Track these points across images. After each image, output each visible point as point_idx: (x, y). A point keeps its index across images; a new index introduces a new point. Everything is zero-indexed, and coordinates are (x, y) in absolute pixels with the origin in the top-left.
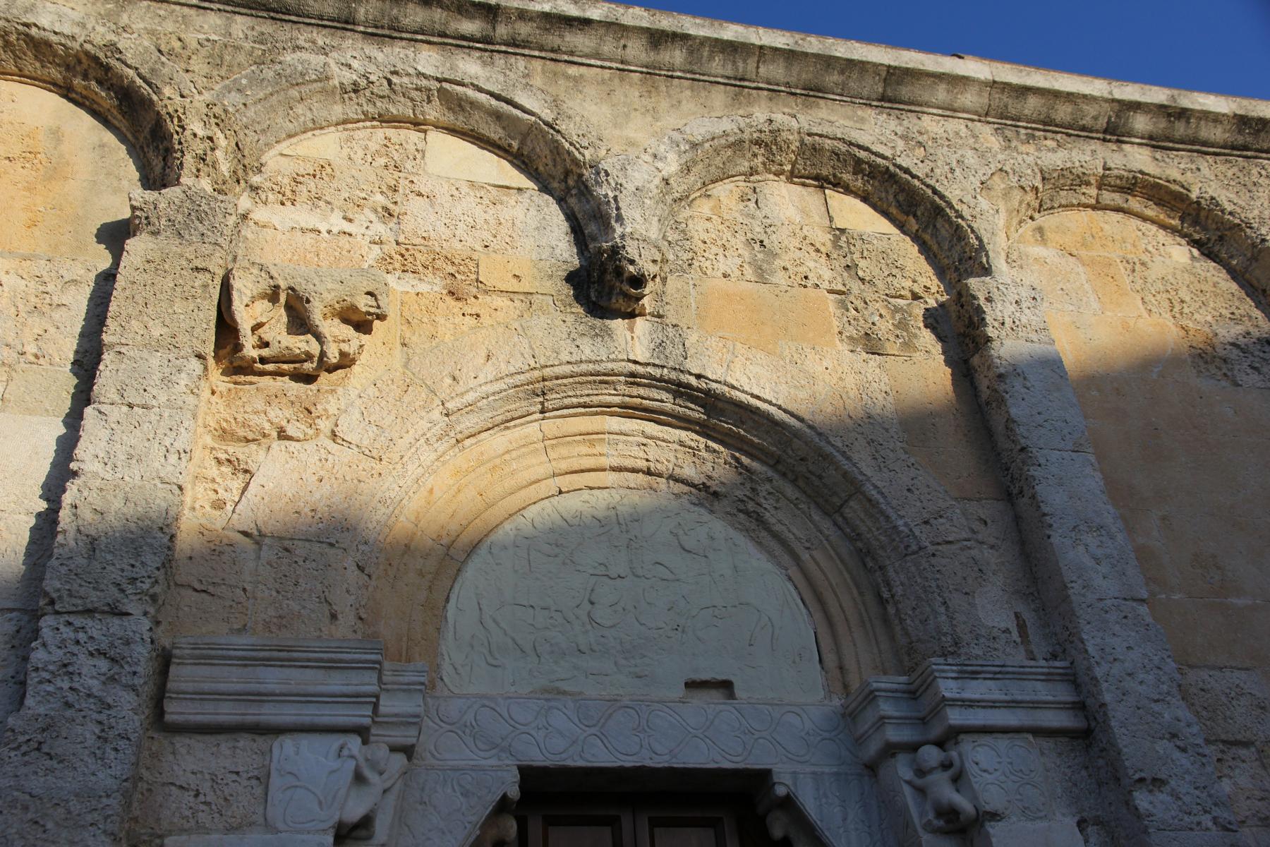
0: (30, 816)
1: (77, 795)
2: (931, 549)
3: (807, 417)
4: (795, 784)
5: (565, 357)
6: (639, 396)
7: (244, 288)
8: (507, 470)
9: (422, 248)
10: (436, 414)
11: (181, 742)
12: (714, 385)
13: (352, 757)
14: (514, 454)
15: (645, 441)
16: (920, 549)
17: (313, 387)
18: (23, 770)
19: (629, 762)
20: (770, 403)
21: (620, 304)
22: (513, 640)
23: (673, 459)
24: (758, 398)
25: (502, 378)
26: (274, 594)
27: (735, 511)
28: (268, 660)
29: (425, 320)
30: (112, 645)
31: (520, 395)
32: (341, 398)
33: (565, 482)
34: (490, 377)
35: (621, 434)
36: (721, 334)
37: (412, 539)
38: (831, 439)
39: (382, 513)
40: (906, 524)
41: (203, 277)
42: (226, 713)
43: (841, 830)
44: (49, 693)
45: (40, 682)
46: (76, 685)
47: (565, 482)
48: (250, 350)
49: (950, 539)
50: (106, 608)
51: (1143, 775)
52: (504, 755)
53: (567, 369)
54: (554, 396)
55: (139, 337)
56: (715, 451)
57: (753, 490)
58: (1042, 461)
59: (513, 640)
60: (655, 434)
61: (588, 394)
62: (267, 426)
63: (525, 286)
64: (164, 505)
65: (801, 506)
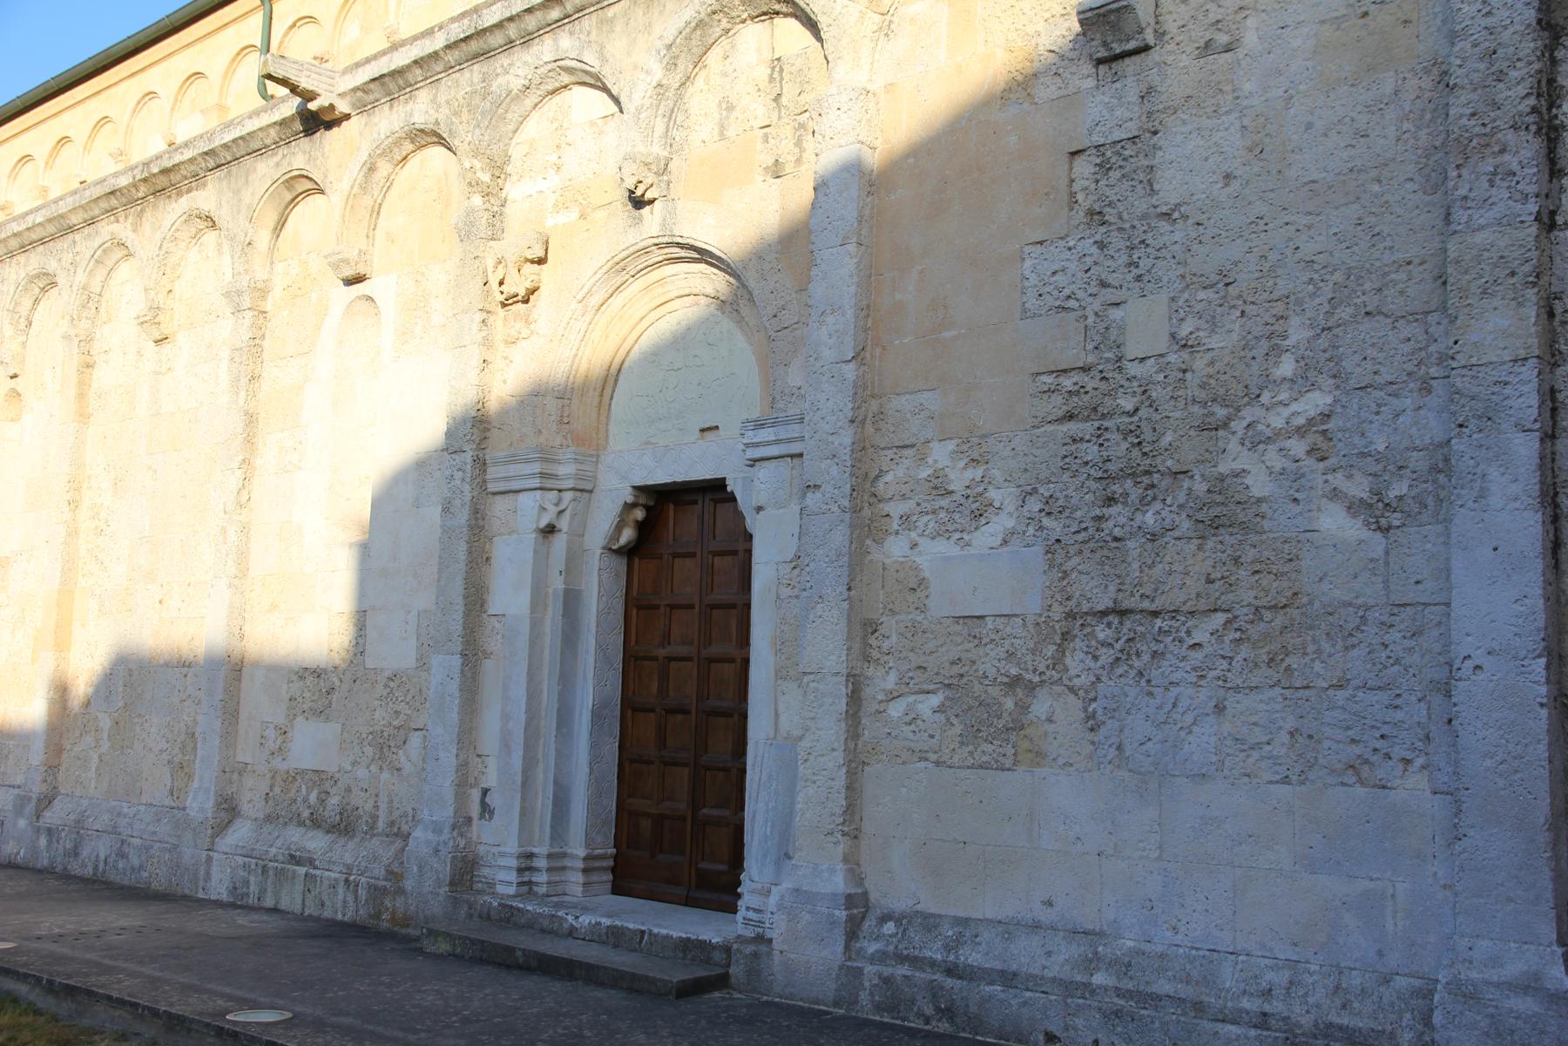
10: (574, 305)
42: (501, 487)
61: (643, 261)
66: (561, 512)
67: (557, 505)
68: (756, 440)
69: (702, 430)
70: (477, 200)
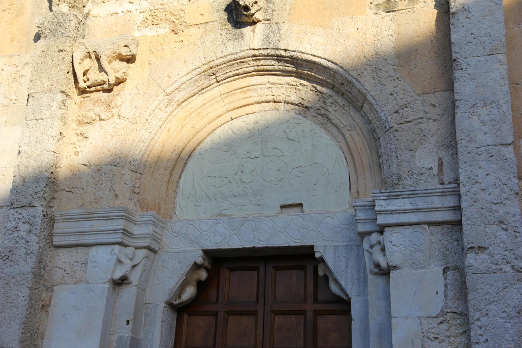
0: (6, 281)
1: (19, 274)
2: (396, 127)
3: (338, 62)
4: (324, 251)
5: (219, 55)
6: (261, 65)
7: (78, 56)
9: (160, 10)
10: (162, 97)
11: (60, 251)
12: (293, 54)
13: (115, 254)
14: (207, 105)
15: (270, 86)
16: (390, 128)
17: (111, 94)
18: (4, 266)
19: (248, 245)
20: (321, 58)
21: (246, 19)
22: (206, 193)
23: (285, 93)
24: (315, 56)
25: (190, 72)
26: (94, 189)
27: (316, 115)
28: (86, 218)
29: (159, 49)
30: (30, 219)
31: (202, 78)
32: (122, 96)
33: (234, 114)
34: (185, 73)
35: (258, 85)
36: (300, 22)
37: (161, 154)
38: (351, 73)
39: (142, 147)
40: (385, 115)
42: (72, 240)
43: (344, 273)
44: (11, 238)
45: (9, 235)
46: (19, 235)
47: (234, 114)
48: (82, 85)
49: (409, 120)
50: (28, 205)
51: (473, 245)
52: (195, 245)
53: (221, 61)
54: (220, 74)
55: (40, 89)
56: (304, 85)
57: (324, 102)
58: (464, 66)
59: (206, 193)
60: (275, 81)
61: (235, 69)
62: (94, 116)
63: (205, 19)
64: (47, 160)
65: (346, 108)
66: (134, 266)
67: (131, 259)
68: (388, 208)
69: (282, 207)
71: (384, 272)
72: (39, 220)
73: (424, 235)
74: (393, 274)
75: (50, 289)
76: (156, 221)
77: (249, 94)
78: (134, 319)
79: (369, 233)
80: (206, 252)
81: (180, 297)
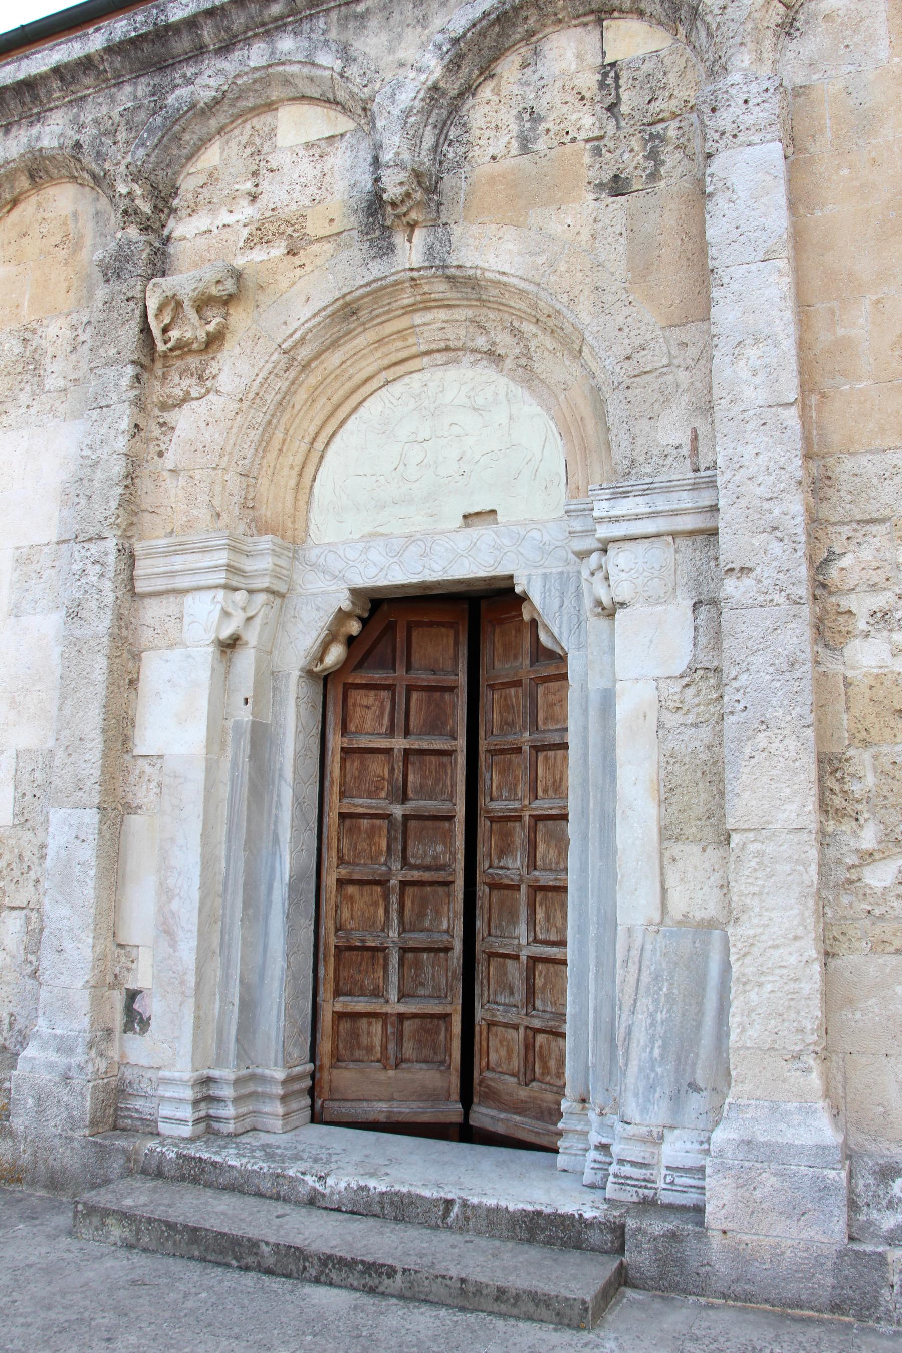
8: (347, 376)
14: (349, 363)
19: (415, 579)
36: (480, 221)
41: (132, 304)
42: (160, 584)
49: (648, 369)
51: (733, 566)
58: (726, 280)
63: (335, 228)
66: (249, 619)
67: (244, 609)
68: (613, 513)
69: (465, 517)
70: (133, 232)
71: (609, 611)
72: (111, 559)
73: (660, 554)
74: (620, 614)
75: (136, 657)
76: (277, 549)
77: (411, 341)
78: (255, 696)
79: (588, 553)
80: (355, 592)
81: (321, 660)
